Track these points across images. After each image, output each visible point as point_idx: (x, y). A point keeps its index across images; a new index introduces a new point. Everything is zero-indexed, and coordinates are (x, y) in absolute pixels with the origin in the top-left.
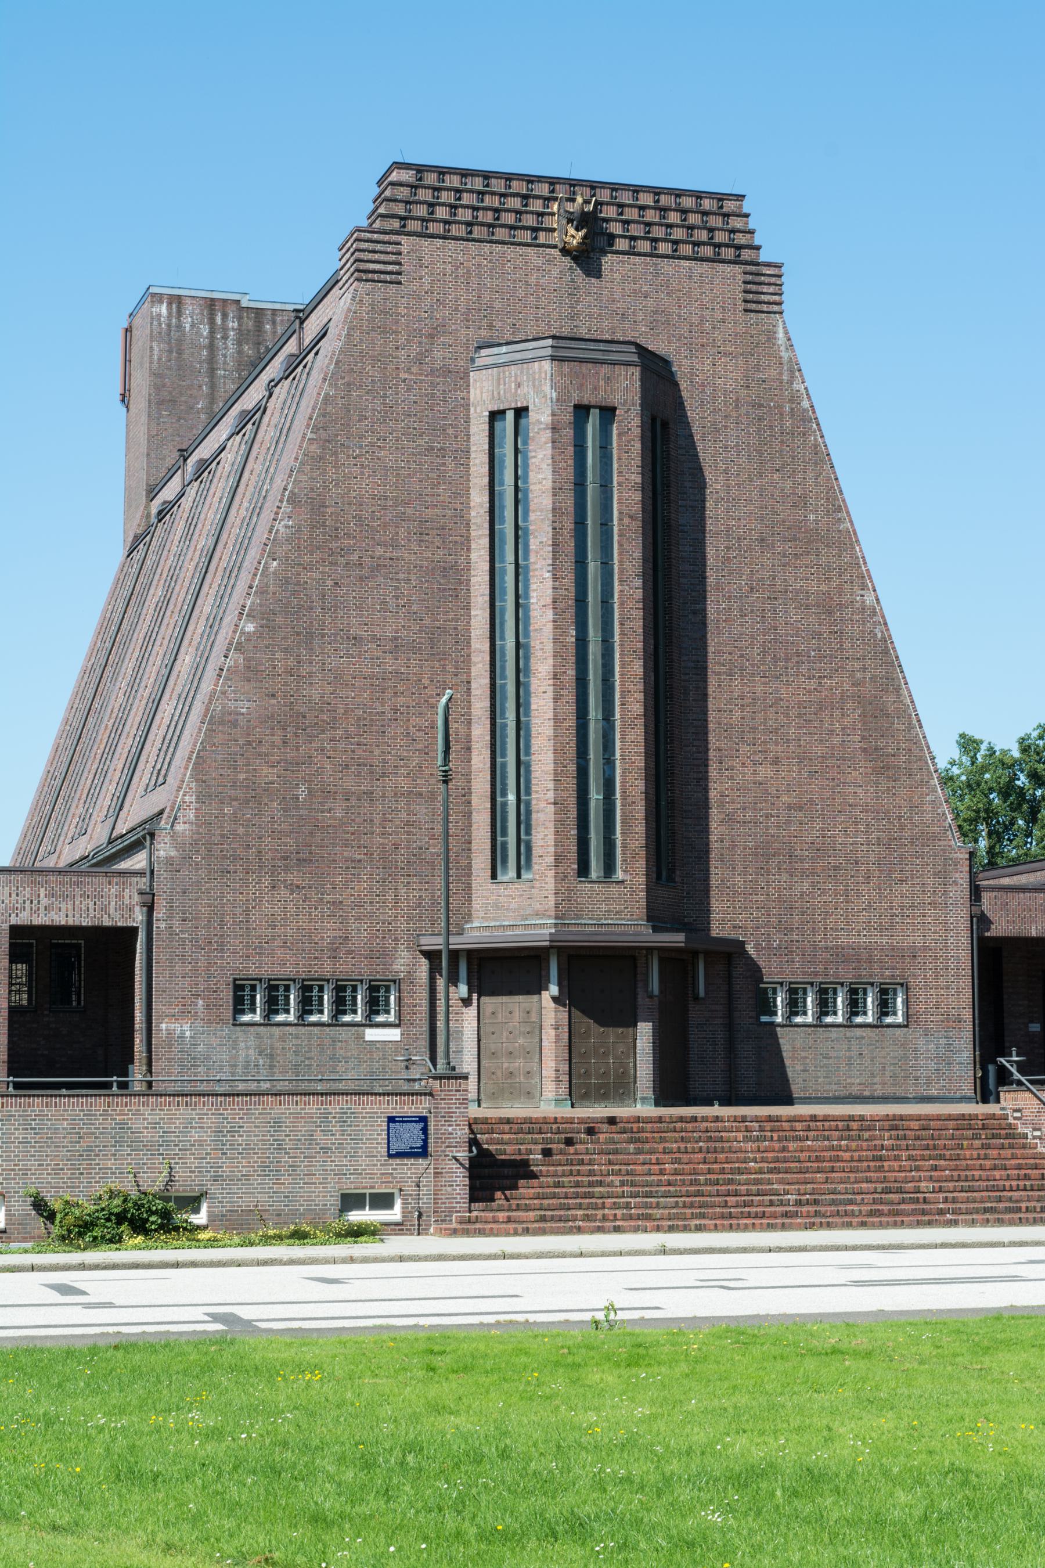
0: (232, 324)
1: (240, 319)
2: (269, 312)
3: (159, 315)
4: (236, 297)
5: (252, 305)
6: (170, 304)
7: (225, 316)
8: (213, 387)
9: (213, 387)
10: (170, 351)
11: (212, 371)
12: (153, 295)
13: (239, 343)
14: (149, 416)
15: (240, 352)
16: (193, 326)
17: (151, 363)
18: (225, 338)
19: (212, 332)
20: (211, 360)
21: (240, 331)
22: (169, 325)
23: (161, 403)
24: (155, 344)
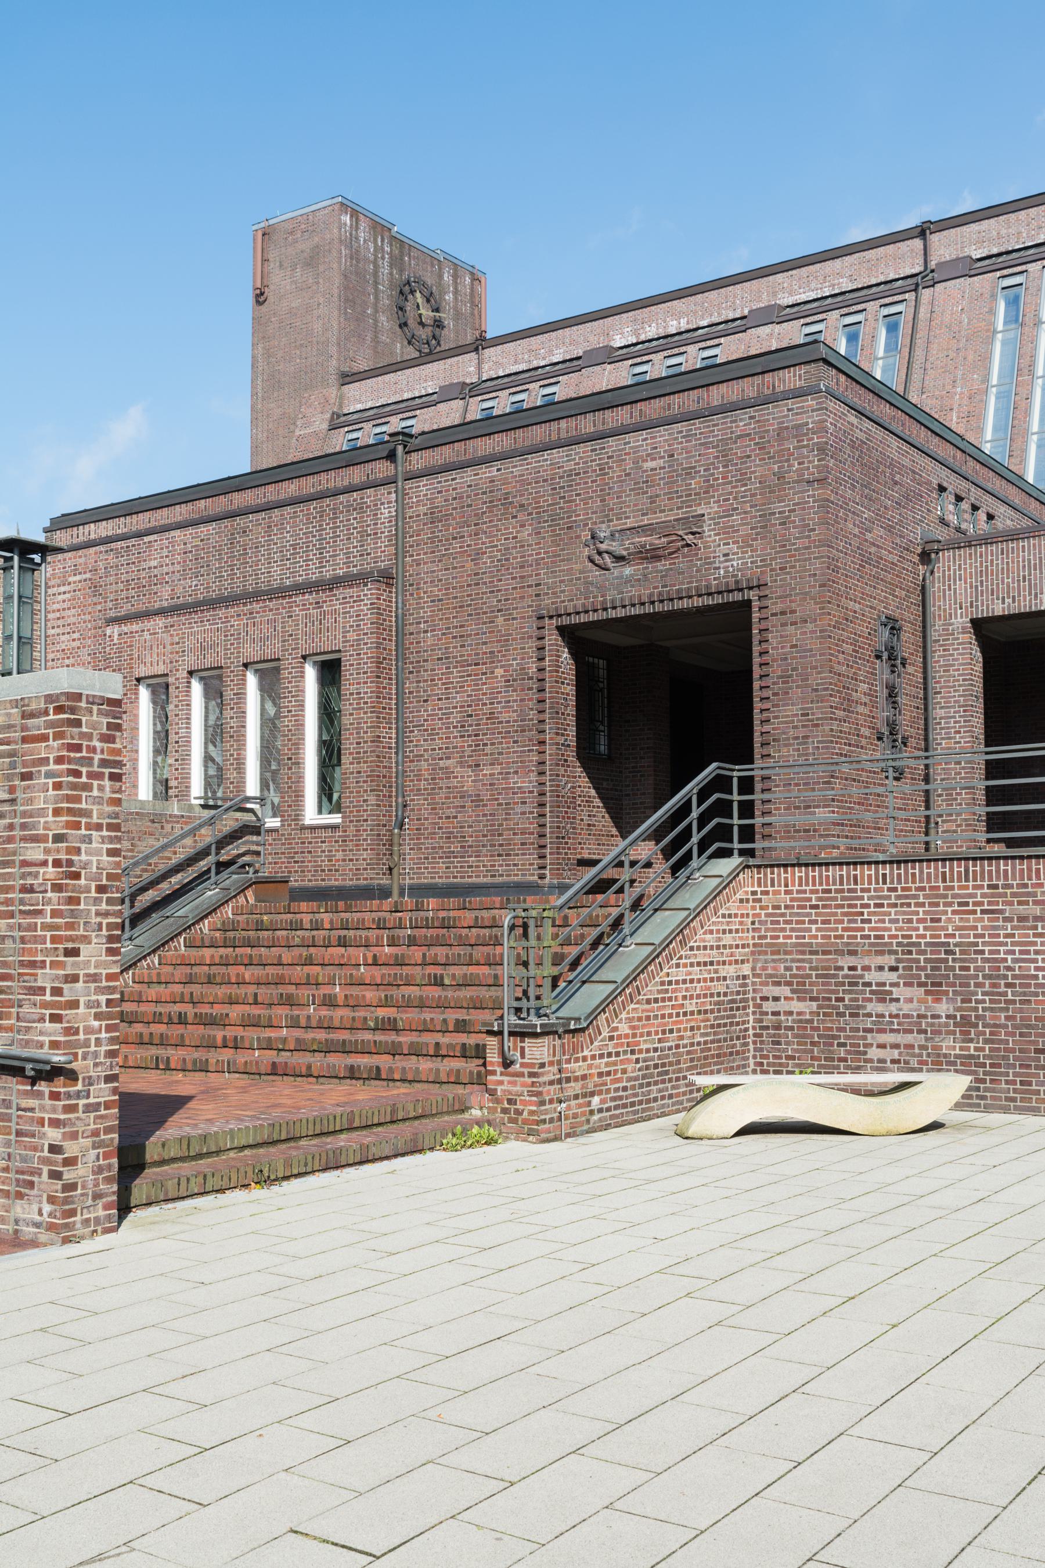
0: (387, 249)
1: (391, 245)
2: (407, 247)
3: (345, 224)
4: (390, 226)
5: (398, 236)
6: (351, 216)
7: (383, 240)
8: (376, 298)
9: (376, 298)
10: (351, 258)
11: (376, 283)
12: (342, 204)
13: (391, 266)
14: (340, 310)
15: (391, 274)
16: (365, 241)
17: (340, 263)
18: (383, 258)
19: (375, 250)
20: (375, 274)
21: (391, 254)
22: (351, 235)
23: (347, 300)
24: (343, 248)
